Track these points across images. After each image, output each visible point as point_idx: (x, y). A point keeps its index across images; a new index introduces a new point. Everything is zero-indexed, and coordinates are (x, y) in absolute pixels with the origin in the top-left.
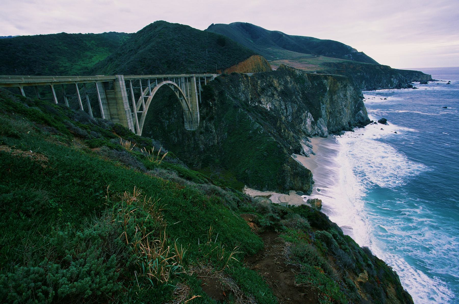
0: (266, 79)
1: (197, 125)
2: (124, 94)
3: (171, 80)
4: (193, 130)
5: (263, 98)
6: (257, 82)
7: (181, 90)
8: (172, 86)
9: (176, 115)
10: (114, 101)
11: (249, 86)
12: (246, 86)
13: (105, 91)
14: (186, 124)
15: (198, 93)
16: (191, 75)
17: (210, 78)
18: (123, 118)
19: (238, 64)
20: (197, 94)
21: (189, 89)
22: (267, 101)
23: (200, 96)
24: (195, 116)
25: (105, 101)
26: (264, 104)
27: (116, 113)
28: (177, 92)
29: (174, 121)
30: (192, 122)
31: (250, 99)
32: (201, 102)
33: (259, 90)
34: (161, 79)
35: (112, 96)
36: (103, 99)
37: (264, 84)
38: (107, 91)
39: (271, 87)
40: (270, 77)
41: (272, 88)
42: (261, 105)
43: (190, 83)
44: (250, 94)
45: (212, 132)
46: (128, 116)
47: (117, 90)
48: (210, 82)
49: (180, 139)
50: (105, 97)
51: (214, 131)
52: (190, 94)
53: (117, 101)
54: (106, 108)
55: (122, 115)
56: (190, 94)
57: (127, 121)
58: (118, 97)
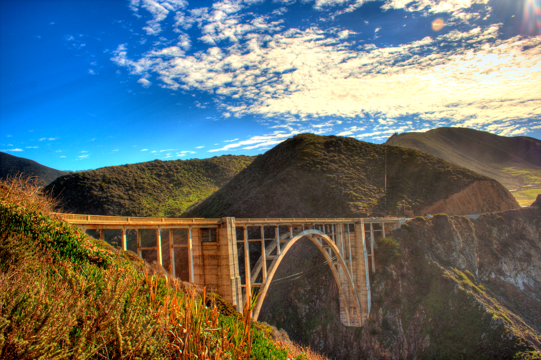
0: (510, 225)
2: (232, 251)
3: (317, 229)
4: (356, 325)
5: (505, 263)
6: (490, 231)
7: (335, 246)
8: (319, 239)
9: (324, 294)
10: (215, 262)
11: (473, 238)
12: (467, 239)
13: (202, 243)
14: (343, 312)
15: (369, 252)
16: (356, 219)
17: (392, 224)
18: (226, 293)
19: (447, 197)
20: (366, 255)
21: (352, 246)
22: (515, 269)
23: (373, 259)
24: (363, 299)
25: (199, 262)
26: (510, 276)
28: (328, 250)
30: (355, 308)
31: (476, 265)
32: (374, 270)
33: (495, 246)
34: (300, 225)
35: (212, 253)
36: (196, 258)
37: (507, 235)
38: (205, 244)
39: (522, 241)
40: (517, 221)
41: (525, 243)
42: (502, 278)
43: (353, 235)
44: (476, 255)
45: (395, 332)
46: (234, 289)
47: (222, 242)
48: (392, 233)
50: (201, 254)
51: (402, 330)
52: (354, 254)
53: (218, 262)
54: (199, 273)
55: (225, 287)
56: (354, 254)
57: (232, 298)
58: (222, 255)
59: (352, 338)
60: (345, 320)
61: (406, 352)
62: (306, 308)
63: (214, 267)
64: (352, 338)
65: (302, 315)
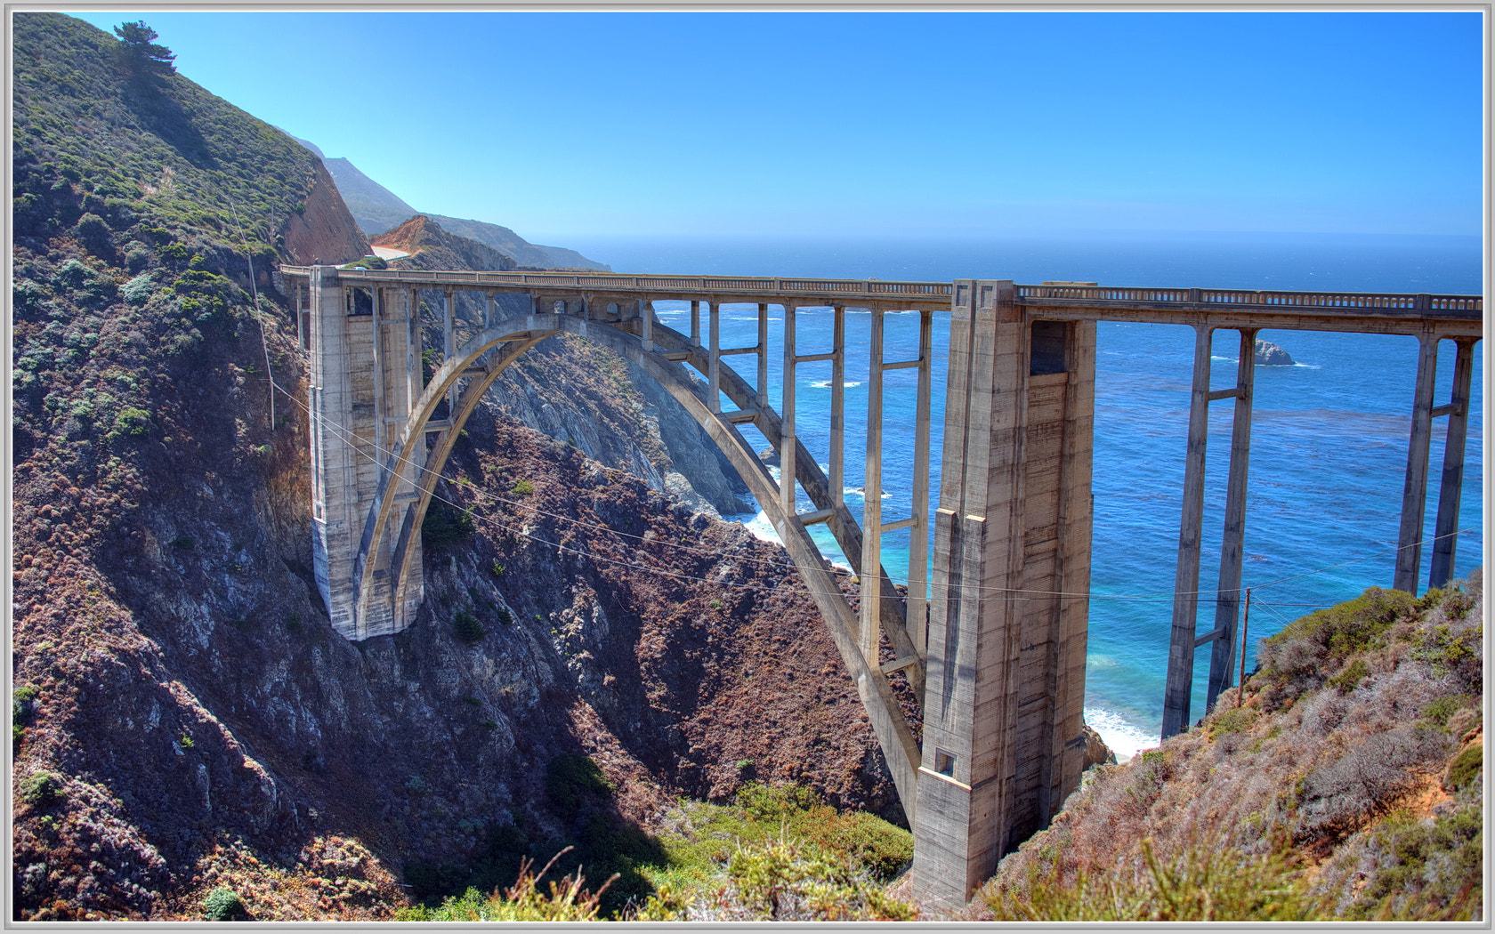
1: (416, 593)
4: (385, 629)
9: (237, 548)
27: (1045, 522)
29: (245, 594)
49: (334, 712)
59: (397, 673)
60: (350, 622)
61: (547, 667)
62: (202, 616)
63: (1048, 466)
64: (397, 673)
65: (198, 646)
